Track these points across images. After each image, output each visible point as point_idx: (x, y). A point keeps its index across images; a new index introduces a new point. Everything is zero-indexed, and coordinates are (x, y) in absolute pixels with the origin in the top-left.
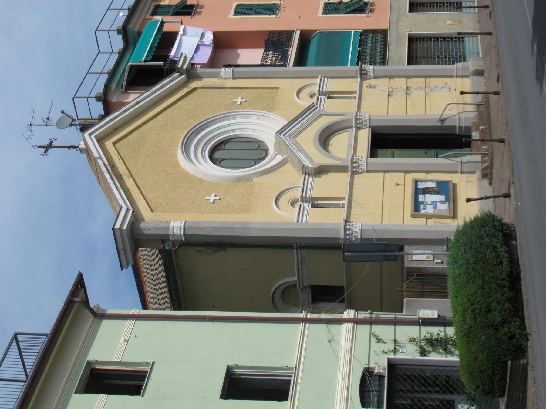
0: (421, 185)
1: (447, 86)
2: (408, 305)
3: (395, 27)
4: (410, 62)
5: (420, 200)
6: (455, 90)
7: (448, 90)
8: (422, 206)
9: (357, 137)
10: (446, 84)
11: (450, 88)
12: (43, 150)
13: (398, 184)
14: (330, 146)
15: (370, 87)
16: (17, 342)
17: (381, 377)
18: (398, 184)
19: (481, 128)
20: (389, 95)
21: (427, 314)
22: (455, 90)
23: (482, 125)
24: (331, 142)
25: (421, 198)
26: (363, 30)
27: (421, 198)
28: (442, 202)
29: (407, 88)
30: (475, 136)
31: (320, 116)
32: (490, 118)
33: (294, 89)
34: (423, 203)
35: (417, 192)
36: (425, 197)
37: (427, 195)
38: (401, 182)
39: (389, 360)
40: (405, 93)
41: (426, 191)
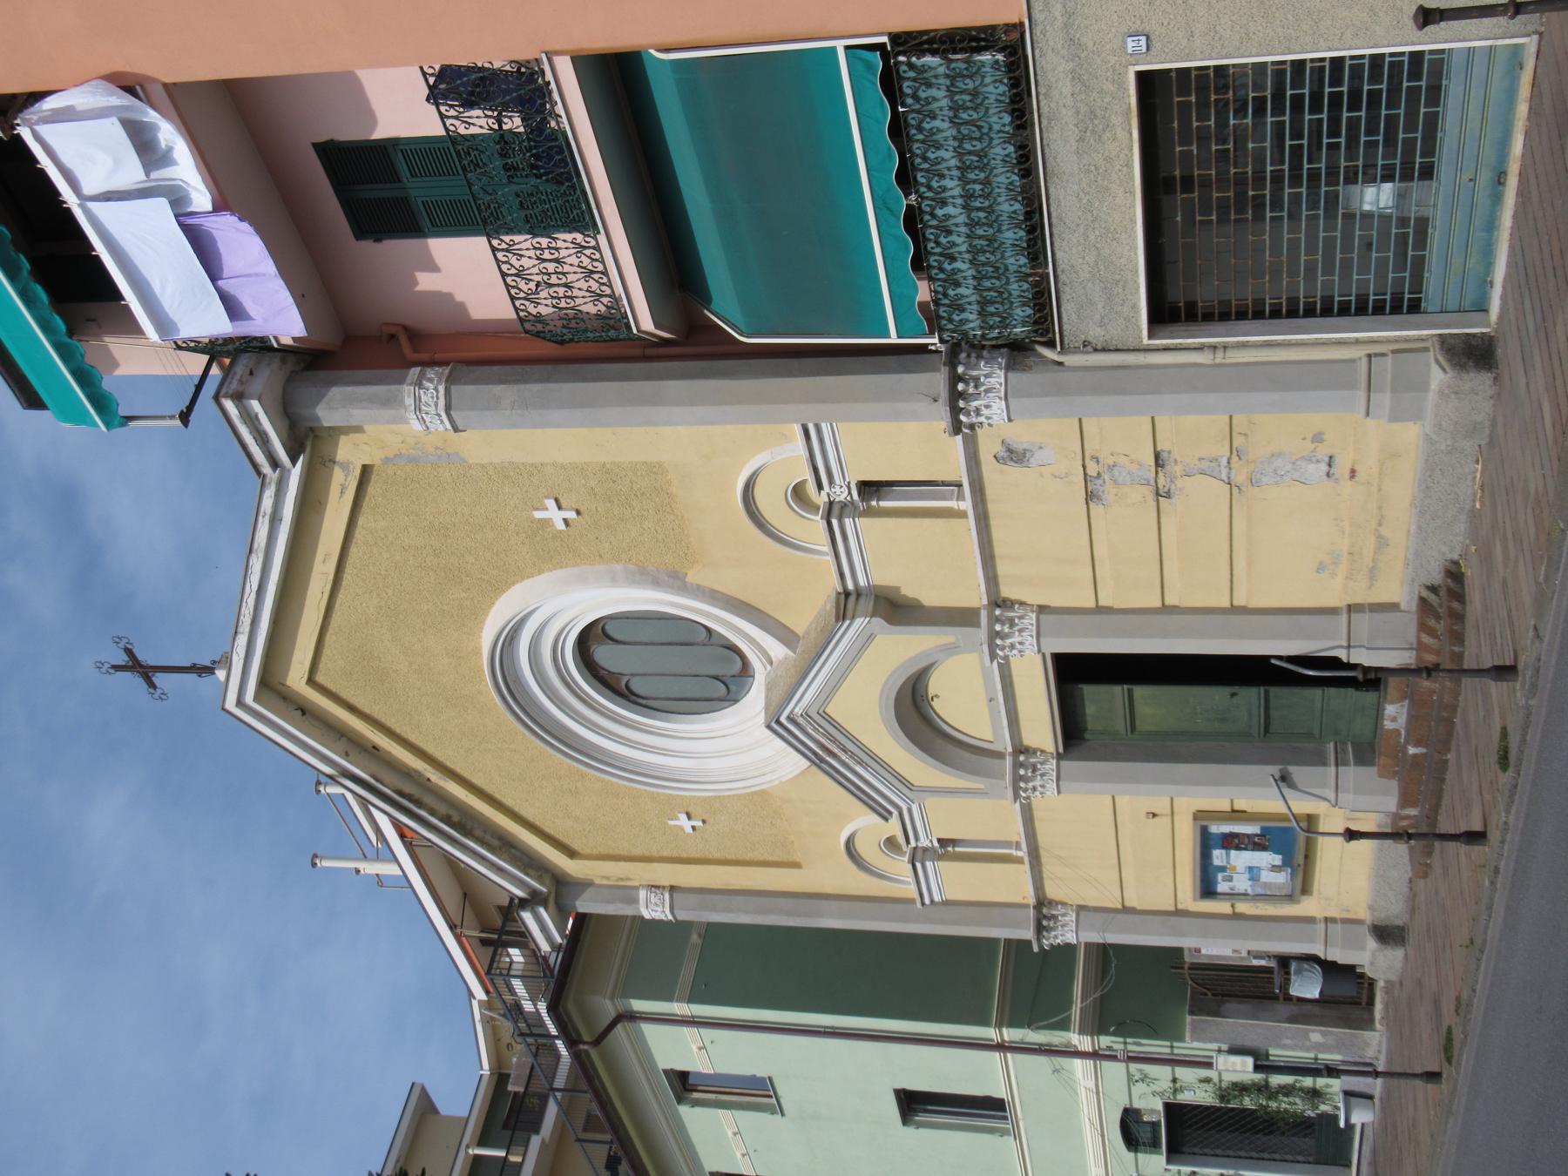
0: (1217, 829)
1: (1323, 452)
2: (1194, 1030)
3: (1059, 23)
4: (1163, 314)
6: (1353, 473)
7: (1324, 467)
8: (1220, 876)
9: (1010, 676)
10: (1318, 438)
13: (1154, 815)
14: (935, 704)
15: (1014, 455)
17: (1155, 1126)
19: (1412, 750)
20: (1090, 496)
22: (1353, 473)
23: (1416, 745)
24: (932, 691)
25: (1218, 856)
26: (895, 38)
28: (1274, 868)
29: (1157, 456)
30: (1394, 719)
31: (871, 637)
32: (1443, 780)
33: (726, 475)
34: (1223, 869)
35: (1206, 842)
36: (1228, 855)
37: (1233, 853)
38: (1161, 805)
40: (1148, 492)
41: (1231, 842)
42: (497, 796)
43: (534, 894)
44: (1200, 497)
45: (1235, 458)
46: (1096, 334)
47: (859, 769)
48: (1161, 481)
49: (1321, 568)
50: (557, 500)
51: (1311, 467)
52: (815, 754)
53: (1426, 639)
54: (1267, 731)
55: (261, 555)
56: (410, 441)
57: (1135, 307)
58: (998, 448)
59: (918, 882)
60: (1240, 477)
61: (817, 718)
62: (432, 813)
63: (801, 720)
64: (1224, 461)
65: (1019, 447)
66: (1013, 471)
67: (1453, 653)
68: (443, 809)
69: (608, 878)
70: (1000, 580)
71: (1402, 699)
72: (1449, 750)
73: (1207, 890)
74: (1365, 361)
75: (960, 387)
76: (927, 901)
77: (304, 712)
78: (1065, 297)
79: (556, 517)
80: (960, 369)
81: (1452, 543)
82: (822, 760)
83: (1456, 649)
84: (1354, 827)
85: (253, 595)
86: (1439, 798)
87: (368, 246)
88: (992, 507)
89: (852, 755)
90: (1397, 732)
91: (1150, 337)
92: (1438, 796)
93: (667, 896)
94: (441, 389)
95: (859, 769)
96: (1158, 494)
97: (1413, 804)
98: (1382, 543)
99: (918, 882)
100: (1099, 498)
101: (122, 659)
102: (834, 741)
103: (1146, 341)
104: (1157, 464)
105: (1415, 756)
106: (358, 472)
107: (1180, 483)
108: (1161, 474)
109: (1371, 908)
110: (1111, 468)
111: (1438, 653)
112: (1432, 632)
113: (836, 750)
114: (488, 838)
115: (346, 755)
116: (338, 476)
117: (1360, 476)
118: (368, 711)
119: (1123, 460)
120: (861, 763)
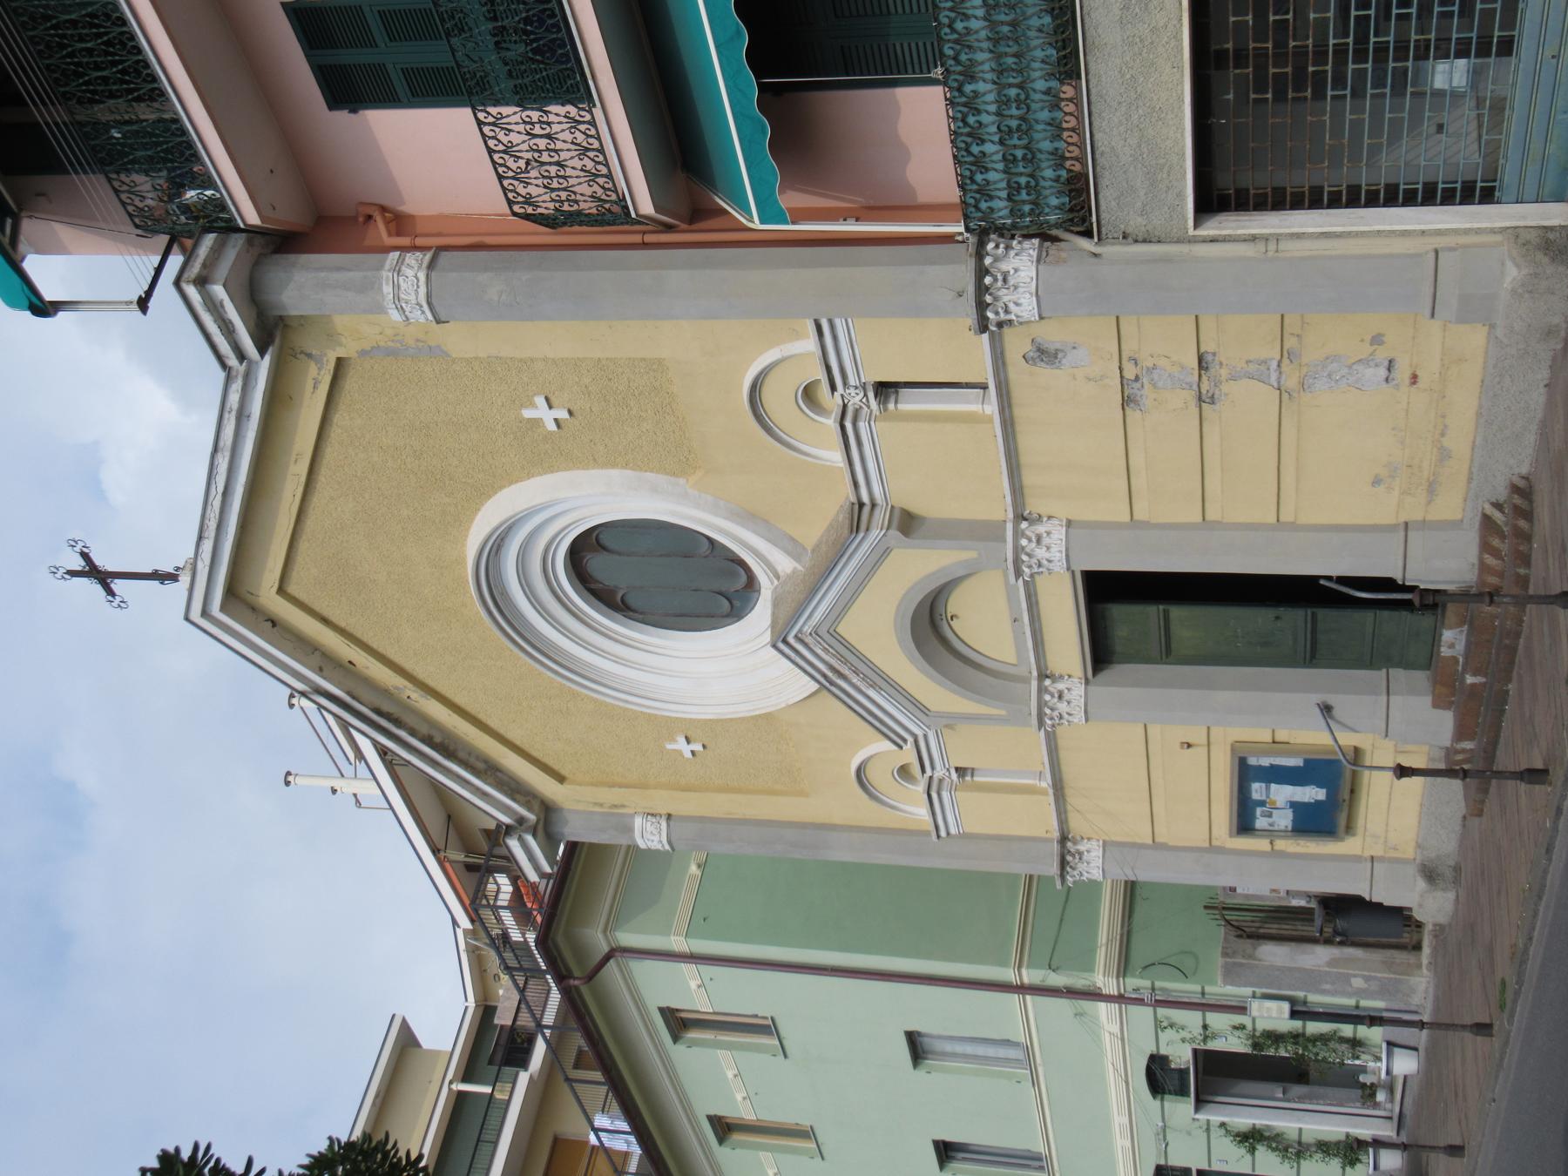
1: (1382, 354)
4: (1210, 201)
5: (1256, 796)
6: (1414, 379)
7: (1383, 372)
8: (1259, 811)
10: (1377, 340)
11: (1390, 365)
12: (78, 564)
13: (1189, 746)
15: (1044, 355)
16: (529, 1007)
17: (1183, 1073)
18: (1189, 746)
19: (1470, 680)
20: (1127, 401)
21: (1269, 1009)
22: (1414, 379)
23: (1474, 675)
24: (951, 610)
25: (1257, 790)
27: (1257, 790)
30: (1452, 646)
31: (887, 551)
32: (1503, 711)
34: (1262, 803)
35: (1245, 773)
36: (1268, 789)
38: (1197, 735)
39: (1195, 1051)
40: (1190, 396)
42: (482, 716)
43: (521, 821)
44: (1247, 401)
45: (1286, 361)
46: (1136, 223)
47: (872, 693)
48: (1205, 387)
49: (1377, 481)
50: (547, 399)
51: (1369, 372)
52: (825, 676)
53: (1490, 560)
54: (1313, 656)
55: (227, 454)
56: (389, 332)
57: (1181, 195)
58: (1027, 347)
59: (934, 814)
60: (1291, 382)
61: (827, 637)
62: (413, 733)
63: (809, 640)
64: (1274, 364)
65: (1052, 348)
66: (1044, 372)
67: (1518, 575)
68: (424, 729)
69: (601, 805)
70: (1026, 491)
71: (1461, 624)
72: (1510, 680)
73: (1244, 825)
74: (1432, 255)
75: (988, 280)
76: (943, 833)
77: (274, 624)
78: (1103, 183)
79: (547, 417)
80: (988, 261)
81: (1519, 461)
82: (832, 683)
83: (1522, 571)
84: (1406, 764)
85: (219, 497)
86: (1497, 737)
87: (342, 116)
88: (1018, 412)
89: (865, 678)
90: (1455, 659)
91: (1196, 227)
92: (1496, 728)
93: (664, 824)
94: (422, 276)
95: (872, 693)
96: (1200, 399)
97: (1471, 739)
98: (1444, 455)
99: (934, 814)
100: (1136, 402)
101: (78, 564)
102: (846, 662)
103: (1191, 232)
104: (1202, 363)
105: (1473, 685)
106: (332, 365)
107: (1225, 388)
108: (1204, 378)
109: (1418, 846)
110: (1150, 370)
111: (1501, 575)
112: (1496, 553)
113: (846, 672)
114: (472, 760)
115: (319, 670)
116: (313, 369)
117: (1422, 383)
118: (343, 624)
119: (1162, 362)
120: (873, 686)
